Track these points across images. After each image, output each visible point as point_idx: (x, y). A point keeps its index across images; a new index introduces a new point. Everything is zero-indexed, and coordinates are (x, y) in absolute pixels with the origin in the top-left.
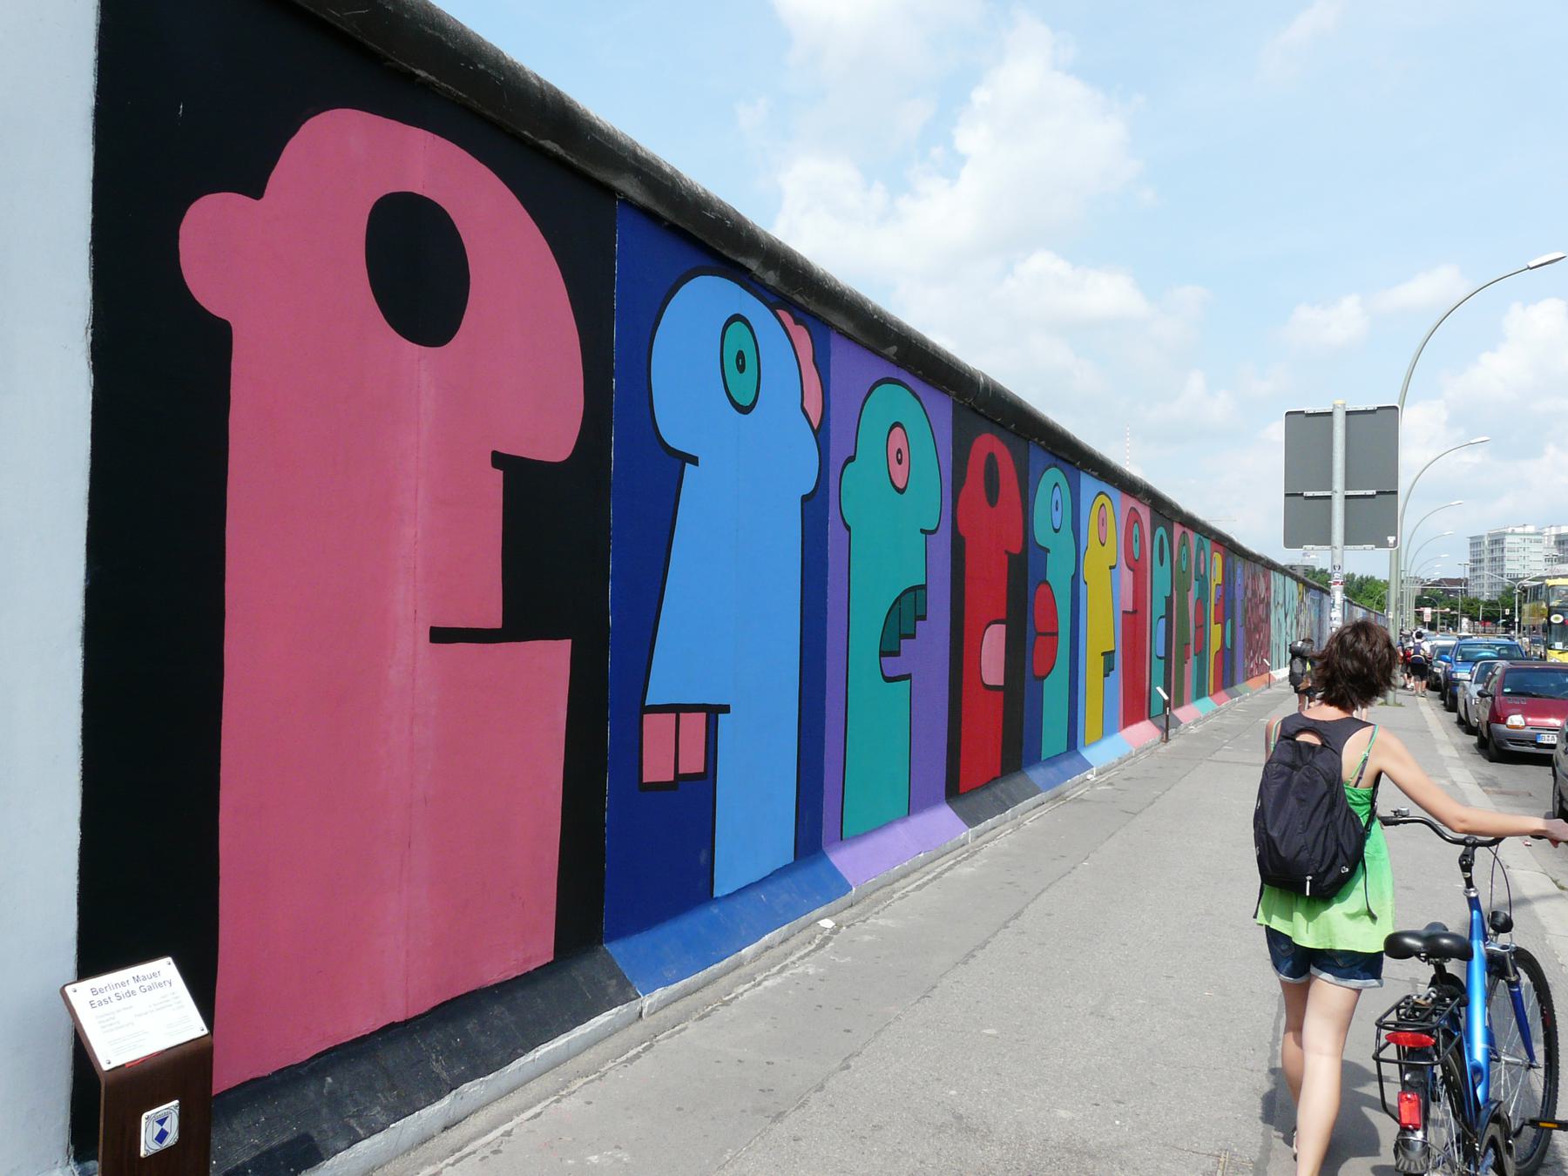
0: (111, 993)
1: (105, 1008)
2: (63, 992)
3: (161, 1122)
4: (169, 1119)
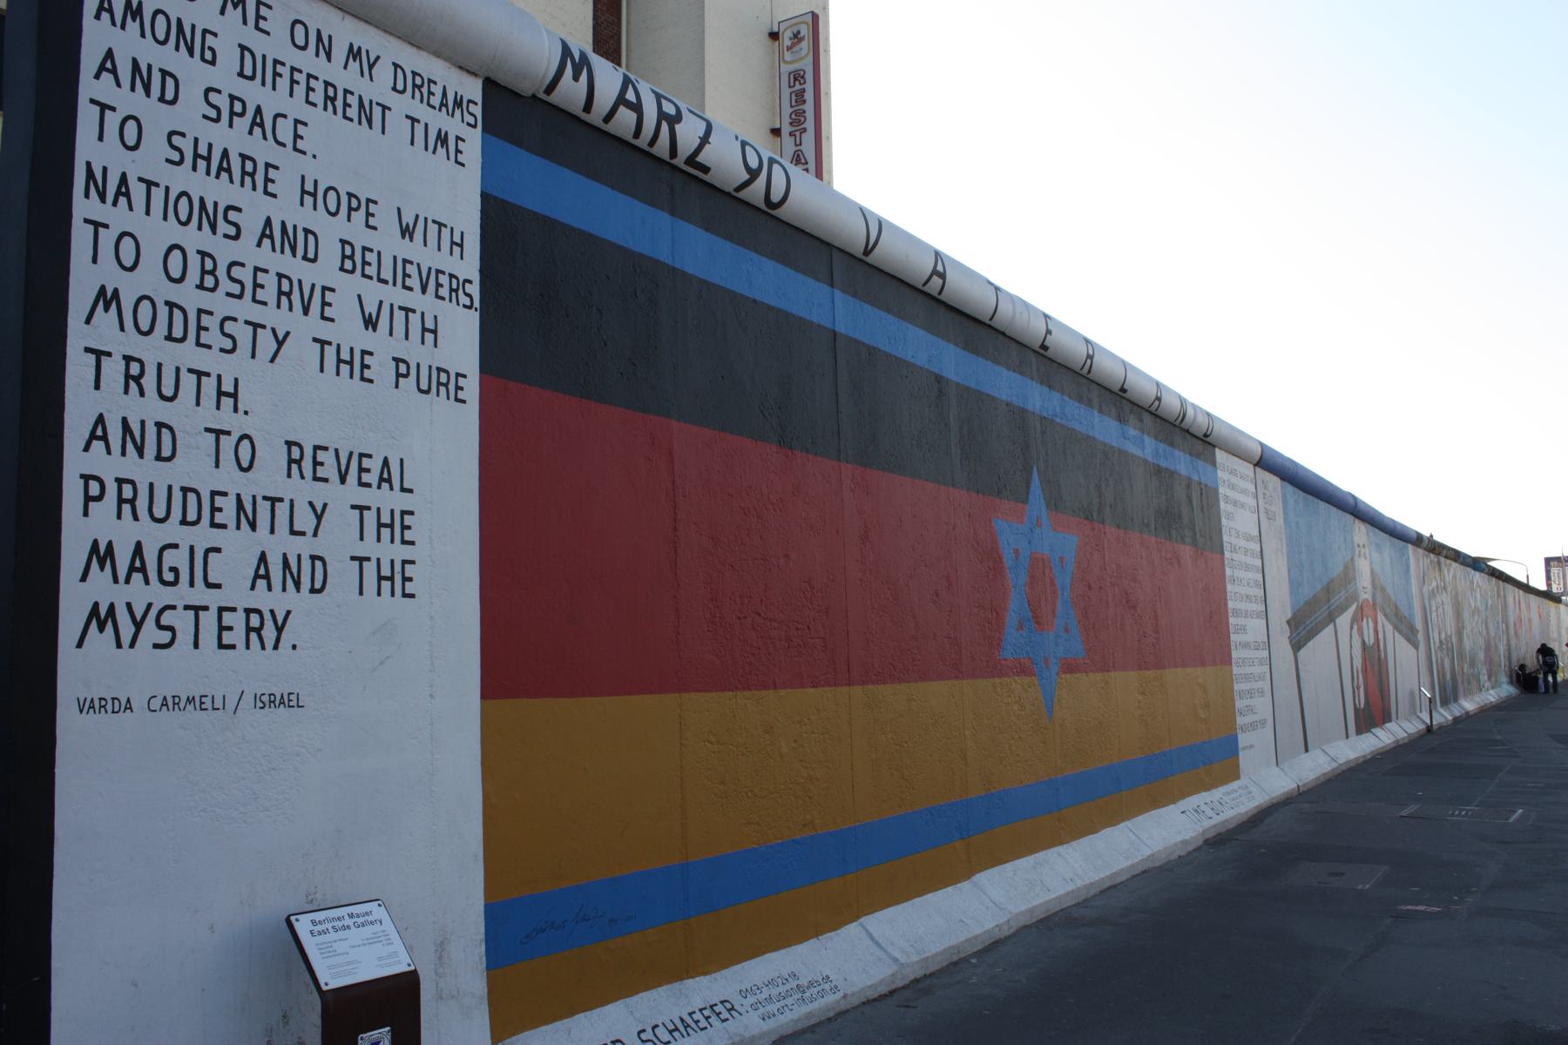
0: (329, 925)
1: (323, 938)
2: (288, 921)
4: (382, 1043)
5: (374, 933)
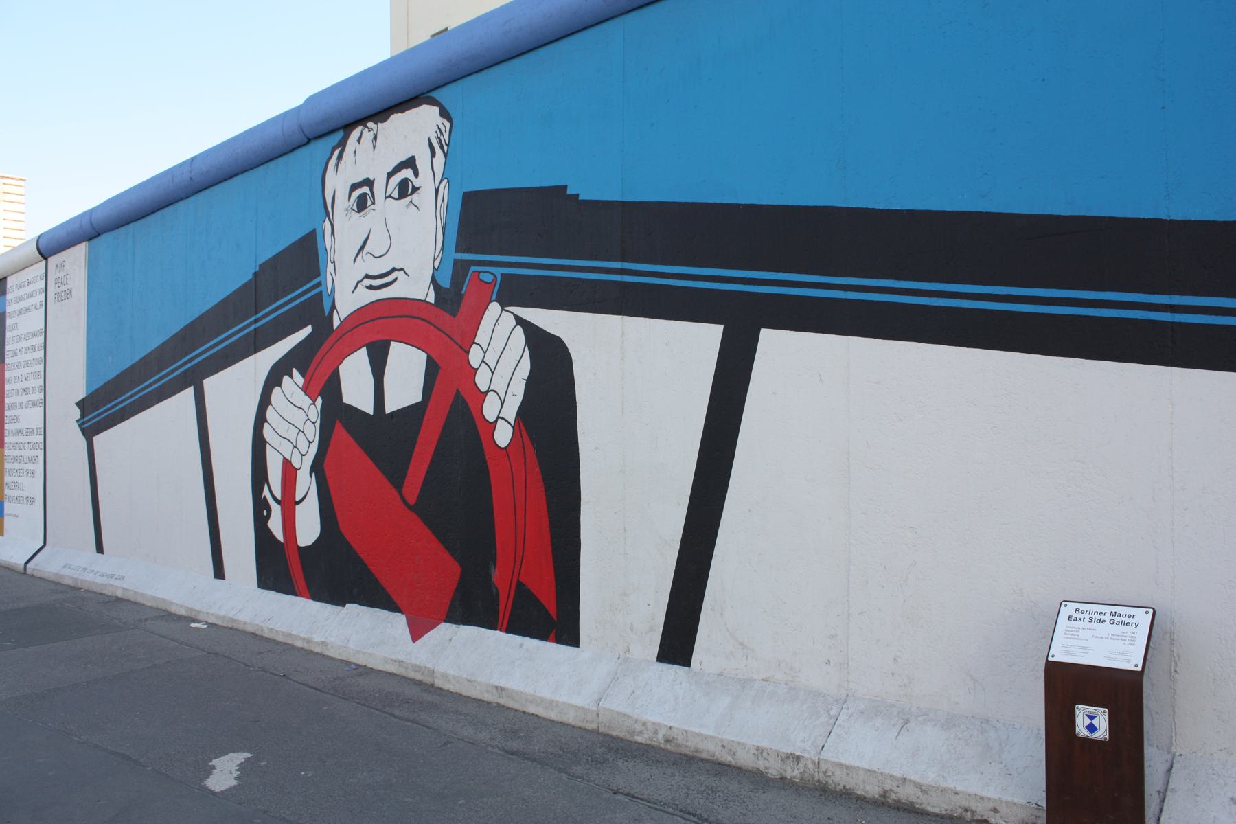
0: (1087, 616)
1: (1077, 624)
3: (1092, 717)
4: (1098, 717)
5: (1124, 633)
